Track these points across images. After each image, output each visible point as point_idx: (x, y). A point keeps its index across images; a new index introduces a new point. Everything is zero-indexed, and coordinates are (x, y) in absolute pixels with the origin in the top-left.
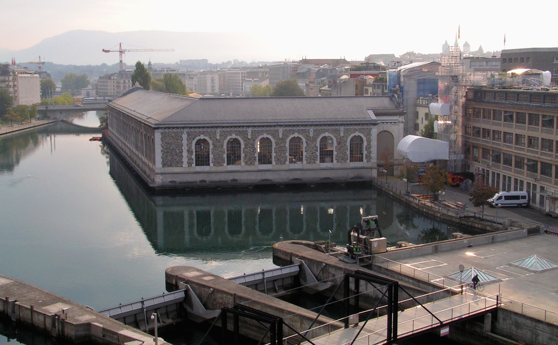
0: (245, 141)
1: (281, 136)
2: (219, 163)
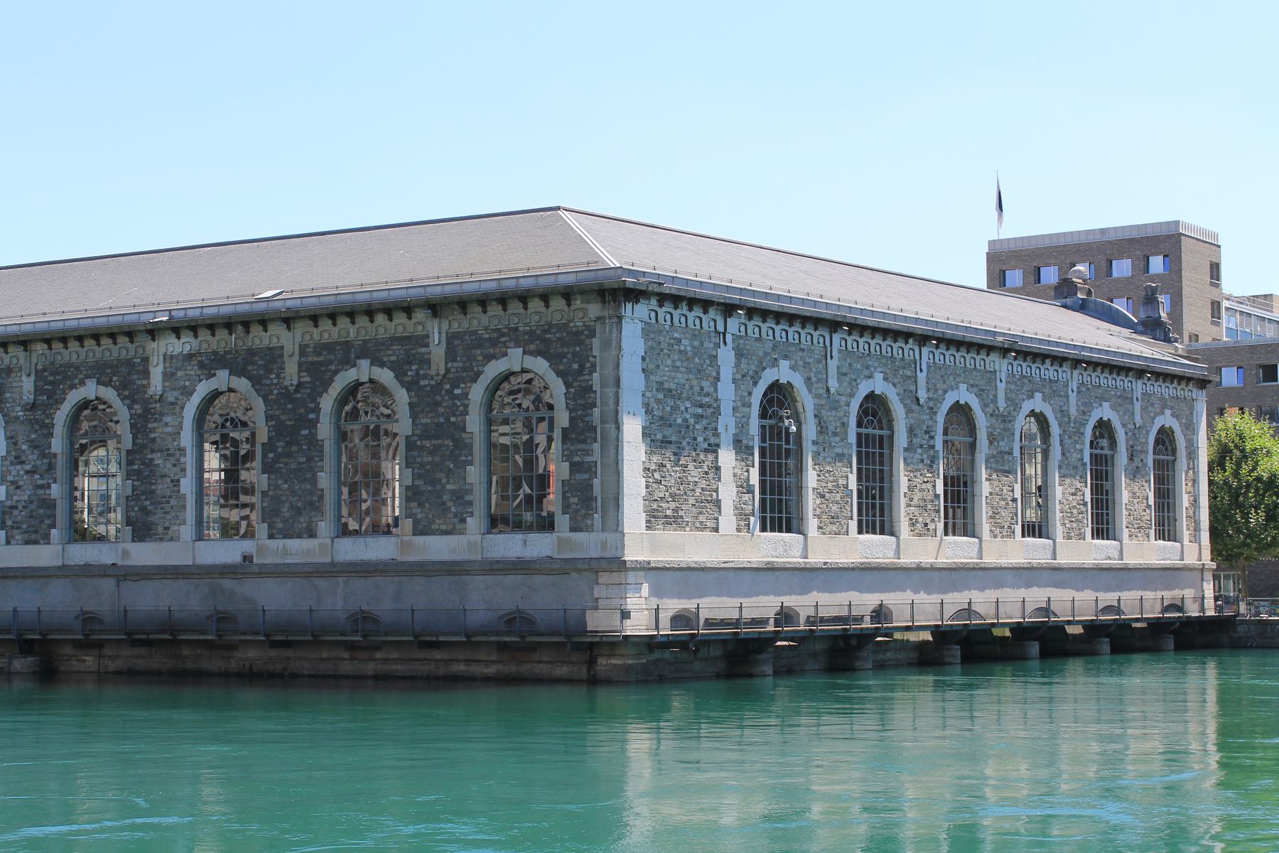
0: (909, 411)
1: (1002, 404)
2: (834, 518)
